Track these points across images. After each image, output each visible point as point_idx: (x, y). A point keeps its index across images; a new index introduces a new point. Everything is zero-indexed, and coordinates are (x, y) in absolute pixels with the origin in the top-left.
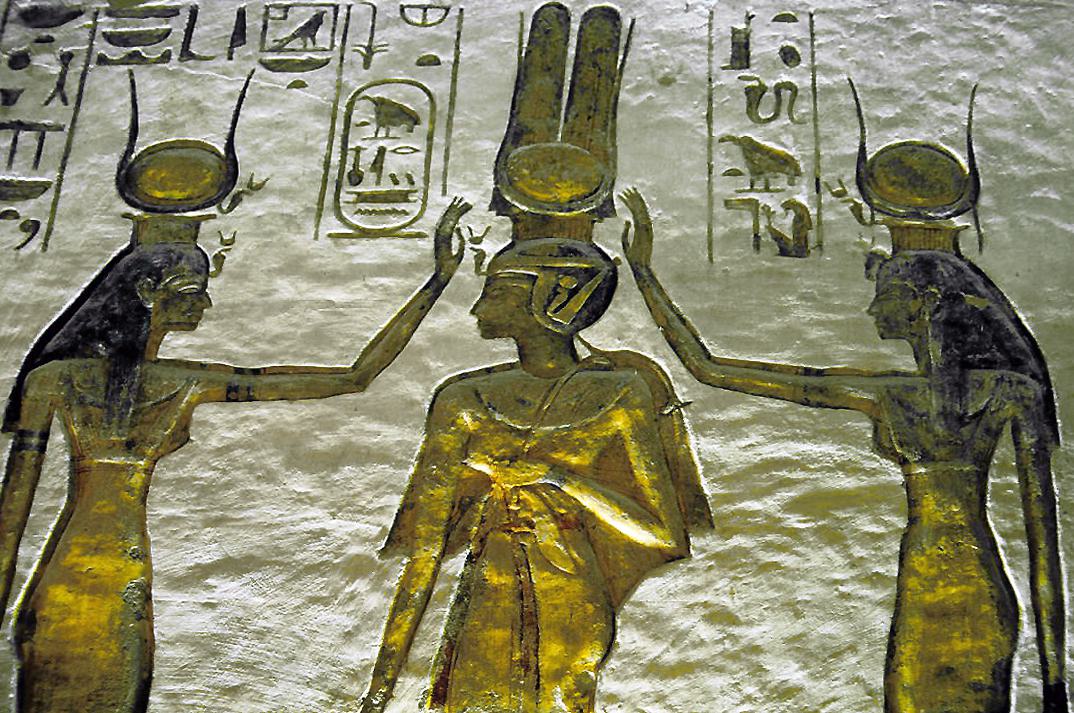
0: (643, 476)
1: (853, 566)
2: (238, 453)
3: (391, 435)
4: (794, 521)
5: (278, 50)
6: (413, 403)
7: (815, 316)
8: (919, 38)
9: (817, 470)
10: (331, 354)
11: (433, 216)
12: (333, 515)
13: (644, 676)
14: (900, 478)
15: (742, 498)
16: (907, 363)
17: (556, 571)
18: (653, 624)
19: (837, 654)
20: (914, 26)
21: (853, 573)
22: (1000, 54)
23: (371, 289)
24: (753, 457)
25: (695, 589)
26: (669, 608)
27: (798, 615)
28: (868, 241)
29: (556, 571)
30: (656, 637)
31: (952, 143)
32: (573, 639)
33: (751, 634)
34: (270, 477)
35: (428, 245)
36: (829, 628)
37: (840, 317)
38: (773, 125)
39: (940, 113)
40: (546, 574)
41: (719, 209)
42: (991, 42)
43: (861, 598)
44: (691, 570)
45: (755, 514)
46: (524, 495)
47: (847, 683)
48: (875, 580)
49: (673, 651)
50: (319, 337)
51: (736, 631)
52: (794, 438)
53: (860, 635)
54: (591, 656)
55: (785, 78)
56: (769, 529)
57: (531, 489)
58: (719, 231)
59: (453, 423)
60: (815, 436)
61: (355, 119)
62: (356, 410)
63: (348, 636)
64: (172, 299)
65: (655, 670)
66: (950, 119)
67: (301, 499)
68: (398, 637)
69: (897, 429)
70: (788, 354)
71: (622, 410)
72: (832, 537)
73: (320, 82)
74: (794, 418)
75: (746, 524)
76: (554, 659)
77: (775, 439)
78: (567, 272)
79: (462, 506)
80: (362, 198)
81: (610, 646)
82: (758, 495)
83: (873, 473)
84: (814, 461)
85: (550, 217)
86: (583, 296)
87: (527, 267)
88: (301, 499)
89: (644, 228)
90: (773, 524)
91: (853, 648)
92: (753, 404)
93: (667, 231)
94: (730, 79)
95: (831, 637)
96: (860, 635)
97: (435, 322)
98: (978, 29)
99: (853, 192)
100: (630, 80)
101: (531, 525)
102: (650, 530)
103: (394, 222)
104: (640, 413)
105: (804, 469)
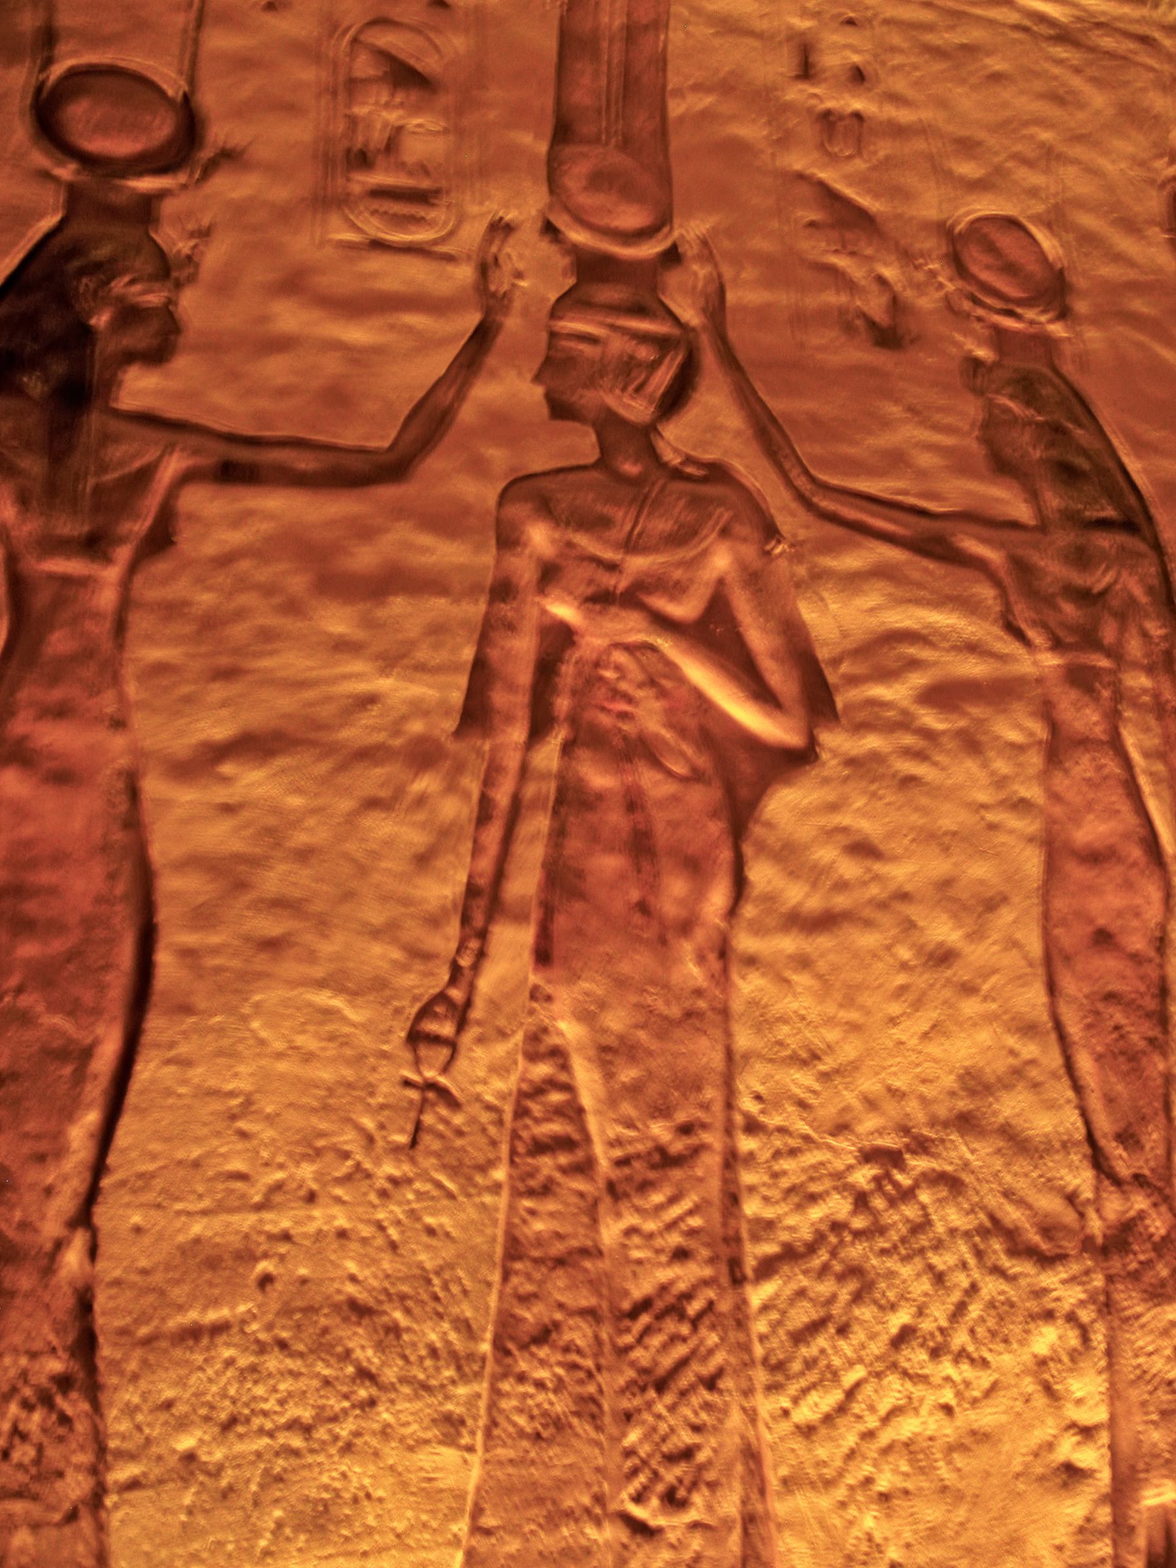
0: (759, 639)
2: (244, 565)
3: (445, 553)
8: (996, 78)
11: (473, 233)
12: (384, 671)
18: (787, 855)
21: (1002, 796)
25: (833, 807)
26: (804, 832)
29: (670, 774)
30: (793, 875)
31: (1031, 218)
33: (900, 873)
34: (293, 607)
35: (465, 273)
36: (979, 871)
40: (659, 776)
43: (1011, 832)
46: (620, 657)
48: (1021, 806)
50: (337, 398)
51: (878, 867)
52: (918, 602)
54: (718, 898)
57: (629, 648)
60: (942, 601)
62: (400, 512)
63: (423, 860)
64: (129, 315)
65: (797, 921)
66: (1033, 192)
67: (342, 646)
68: (486, 864)
69: (1023, 599)
72: (971, 744)
74: (916, 575)
75: (872, 718)
76: (681, 902)
82: (886, 675)
84: (944, 637)
86: (663, 378)
88: (342, 646)
90: (905, 723)
91: (1005, 899)
94: (796, 93)
95: (982, 882)
97: (487, 392)
101: (630, 700)
102: (769, 715)
103: (420, 236)
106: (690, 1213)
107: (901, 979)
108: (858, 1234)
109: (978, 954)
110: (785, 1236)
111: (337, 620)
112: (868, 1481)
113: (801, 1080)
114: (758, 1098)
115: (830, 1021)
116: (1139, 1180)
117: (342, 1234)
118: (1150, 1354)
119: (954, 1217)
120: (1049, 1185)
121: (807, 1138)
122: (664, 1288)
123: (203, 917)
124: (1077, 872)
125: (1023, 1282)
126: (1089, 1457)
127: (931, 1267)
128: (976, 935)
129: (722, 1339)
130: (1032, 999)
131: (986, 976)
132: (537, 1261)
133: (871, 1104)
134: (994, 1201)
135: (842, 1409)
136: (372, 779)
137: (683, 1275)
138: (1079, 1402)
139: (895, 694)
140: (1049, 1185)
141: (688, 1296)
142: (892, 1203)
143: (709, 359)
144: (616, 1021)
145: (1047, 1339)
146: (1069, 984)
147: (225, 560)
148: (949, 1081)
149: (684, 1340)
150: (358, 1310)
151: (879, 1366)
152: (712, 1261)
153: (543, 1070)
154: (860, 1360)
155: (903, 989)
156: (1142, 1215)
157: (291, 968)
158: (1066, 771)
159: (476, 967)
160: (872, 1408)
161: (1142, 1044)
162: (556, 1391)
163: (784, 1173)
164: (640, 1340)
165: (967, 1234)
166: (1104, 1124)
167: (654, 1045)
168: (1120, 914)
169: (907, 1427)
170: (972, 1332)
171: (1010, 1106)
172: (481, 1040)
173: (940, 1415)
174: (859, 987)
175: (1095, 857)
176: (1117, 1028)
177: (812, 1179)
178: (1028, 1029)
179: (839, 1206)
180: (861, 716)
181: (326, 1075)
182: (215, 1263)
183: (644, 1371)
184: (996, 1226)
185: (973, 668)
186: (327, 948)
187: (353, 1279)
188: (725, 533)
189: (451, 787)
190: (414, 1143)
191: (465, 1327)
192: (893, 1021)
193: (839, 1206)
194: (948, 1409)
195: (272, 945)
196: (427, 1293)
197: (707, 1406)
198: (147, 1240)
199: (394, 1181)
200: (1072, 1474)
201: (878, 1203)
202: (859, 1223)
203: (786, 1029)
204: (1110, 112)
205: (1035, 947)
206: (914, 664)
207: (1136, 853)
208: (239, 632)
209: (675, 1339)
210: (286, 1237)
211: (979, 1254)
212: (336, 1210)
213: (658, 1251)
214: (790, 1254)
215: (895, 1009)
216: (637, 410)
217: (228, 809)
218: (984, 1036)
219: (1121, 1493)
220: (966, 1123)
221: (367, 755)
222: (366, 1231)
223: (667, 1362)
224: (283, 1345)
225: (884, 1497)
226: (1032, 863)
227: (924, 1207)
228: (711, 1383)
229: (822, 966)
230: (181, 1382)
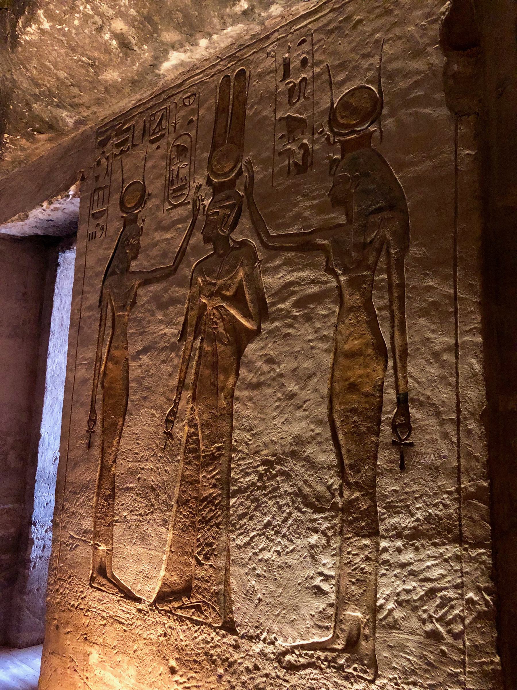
1: (316, 332)
2: (146, 305)
4: (295, 312)
5: (153, 134)
6: (187, 277)
7: (308, 203)
9: (304, 285)
10: (167, 261)
13: (246, 389)
14: (335, 284)
15: (278, 303)
16: (342, 219)
17: (223, 343)
19: (309, 377)
20: (355, 17)
21: (316, 336)
22: (396, 12)
23: (176, 230)
24: (282, 282)
25: (263, 348)
26: (255, 357)
27: (296, 358)
28: (331, 155)
30: (250, 371)
32: (227, 372)
36: (306, 364)
37: (317, 201)
38: (297, 105)
39: (365, 67)
41: (277, 158)
44: (261, 339)
45: (282, 310)
47: (313, 392)
48: (324, 338)
49: (256, 377)
50: (164, 255)
53: (318, 367)
55: (303, 76)
56: (286, 317)
57: (216, 308)
58: (277, 169)
59: (196, 284)
61: (173, 157)
67: (161, 322)
70: (296, 227)
71: (241, 269)
72: (308, 318)
73: (163, 143)
74: (296, 260)
76: (222, 382)
77: (290, 272)
78: (227, 207)
79: (199, 318)
80: (174, 191)
81: (238, 374)
82: (283, 300)
83: (324, 283)
84: (304, 280)
85: (224, 182)
87: (216, 208)
88: (161, 322)
89: (252, 178)
90: (288, 315)
91: (314, 374)
92: (282, 256)
93: (258, 177)
95: (307, 368)
96: (318, 367)
97: (192, 241)
99: (326, 129)
100: (250, 101)
104: (246, 268)
105: (300, 285)
106: (217, 474)
107: (277, 404)
108: (259, 488)
109: (303, 395)
110: (239, 485)
111: (160, 316)
112: (254, 569)
113: (247, 436)
114: (236, 441)
115: (256, 418)
116: (357, 486)
117: (152, 469)
118: (354, 555)
119: (286, 487)
120: (321, 481)
121: (247, 454)
122: (211, 494)
123: (135, 393)
124: (344, 362)
125: (307, 515)
126: (325, 587)
127: (278, 503)
128: (302, 388)
129: (222, 513)
130: (322, 411)
131: (305, 402)
132: (187, 482)
133: (266, 445)
134: (300, 483)
135: (249, 544)
136: (163, 356)
137: (216, 492)
138: (324, 565)
139: (285, 305)
140: (321, 481)
141: (215, 498)
142: (268, 480)
143: (245, 207)
144: (205, 417)
145: (314, 539)
146: (337, 406)
147: (143, 305)
148: (290, 439)
149: (213, 511)
150: (153, 489)
151: (260, 533)
152: (221, 489)
153: (192, 430)
154: (255, 529)
155: (278, 407)
156: (357, 499)
157: (147, 404)
158: (343, 322)
159: (178, 402)
160: (257, 545)
161: (364, 430)
162: (187, 518)
163: (241, 465)
164: (203, 509)
165: (290, 494)
166: (346, 461)
167: (213, 424)
168: (360, 377)
169: (267, 555)
170: (289, 528)
171: (310, 450)
172: (178, 422)
173: (276, 554)
174: (264, 407)
175: (352, 355)
176: (355, 422)
177: (247, 468)
178: (319, 422)
179: (254, 478)
180: (274, 316)
181: (151, 430)
182: (132, 473)
183: (203, 517)
184: (300, 493)
185: (314, 289)
186: (153, 399)
187: (153, 481)
188: (242, 265)
189: (177, 355)
190: (164, 448)
191: (169, 496)
192: (274, 418)
193: (254, 478)
194: (278, 552)
195: (145, 398)
196: (164, 486)
197: (216, 532)
198: (123, 466)
199: (160, 457)
200: (319, 591)
201: (265, 478)
202: (259, 484)
203: (244, 419)
205: (325, 391)
206: (294, 293)
207: (370, 351)
208: (144, 322)
209: (211, 510)
210: (142, 469)
211: (294, 502)
212: (151, 464)
213: (210, 484)
214: (240, 491)
215: (275, 414)
216: (223, 232)
217: (141, 366)
218: (303, 424)
219: (339, 606)
220: (294, 455)
221: (163, 349)
222: (155, 469)
223: (209, 517)
224: (140, 494)
225: (258, 576)
226: (328, 360)
227: (278, 482)
228: (218, 525)
229: (255, 400)
230: (125, 500)
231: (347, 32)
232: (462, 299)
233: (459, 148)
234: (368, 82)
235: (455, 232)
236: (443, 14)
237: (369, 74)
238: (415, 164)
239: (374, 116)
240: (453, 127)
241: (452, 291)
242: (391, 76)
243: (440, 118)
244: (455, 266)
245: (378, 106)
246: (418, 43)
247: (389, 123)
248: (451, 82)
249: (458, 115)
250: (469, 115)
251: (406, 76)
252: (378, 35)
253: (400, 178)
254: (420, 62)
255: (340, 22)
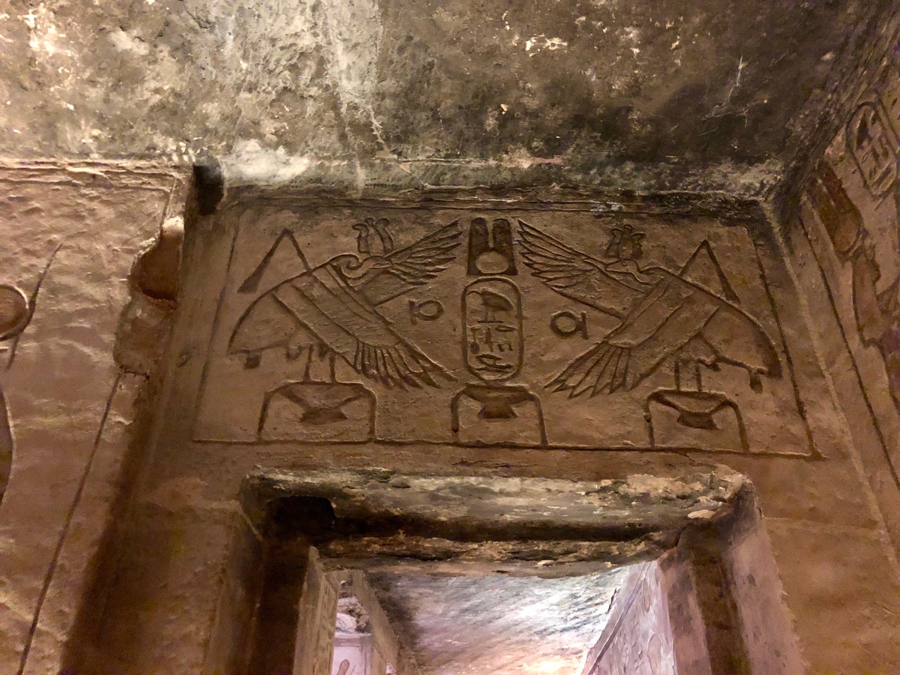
22: (88, 222)
39: (25, 264)
42: (84, 214)
98: (78, 204)
204: (113, 216)
231: (15, 214)
232: (41, 633)
233: (112, 411)
234: (20, 284)
235: (67, 526)
236: (144, 248)
237: (26, 276)
238: (45, 414)
239: (10, 331)
240: (112, 382)
241: (30, 618)
242: (55, 290)
243: (100, 365)
244: (48, 579)
245: (24, 320)
246: (103, 267)
247: (29, 347)
248: (128, 327)
249: (123, 368)
250: (136, 373)
251: (74, 298)
252: (55, 236)
253: (15, 426)
254: (98, 289)
255: (11, 199)
